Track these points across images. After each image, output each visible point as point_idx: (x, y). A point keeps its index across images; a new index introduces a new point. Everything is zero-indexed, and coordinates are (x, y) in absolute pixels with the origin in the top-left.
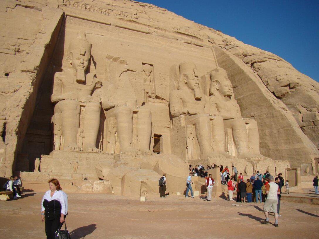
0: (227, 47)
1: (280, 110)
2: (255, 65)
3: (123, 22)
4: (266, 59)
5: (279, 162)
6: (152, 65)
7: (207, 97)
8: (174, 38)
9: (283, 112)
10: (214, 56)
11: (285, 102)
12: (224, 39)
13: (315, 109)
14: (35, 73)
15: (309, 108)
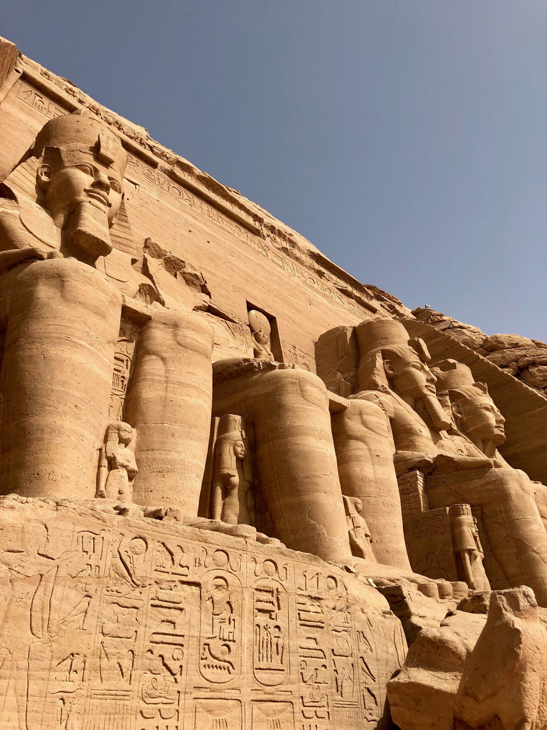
2: (534, 370)
6: (272, 319)
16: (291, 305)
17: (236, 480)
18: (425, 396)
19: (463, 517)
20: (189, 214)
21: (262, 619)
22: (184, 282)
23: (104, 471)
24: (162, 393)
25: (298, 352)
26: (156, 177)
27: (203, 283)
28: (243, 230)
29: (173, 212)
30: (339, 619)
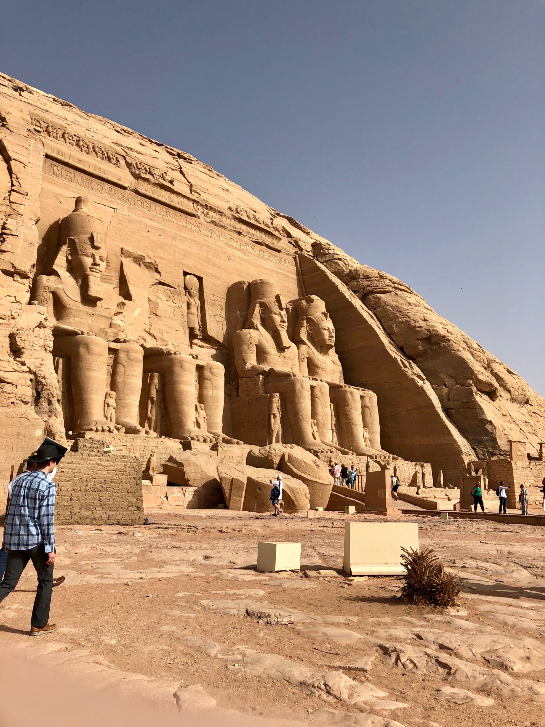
0: (320, 259)
1: (415, 378)
2: (371, 296)
3: (149, 186)
4: (391, 289)
5: (416, 465)
6: (200, 279)
7: (293, 346)
8: (234, 231)
9: (420, 383)
10: (297, 271)
11: (420, 364)
12: (316, 242)
13: (471, 382)
14: (29, 278)
15: (459, 379)
16: (215, 265)
17: (155, 399)
18: (278, 330)
19: (274, 399)
20: (148, 218)
21: (141, 452)
22: (145, 268)
23: (106, 408)
24: (123, 379)
25: (216, 298)
26: (126, 197)
27: (156, 266)
28: (184, 216)
29: (137, 220)
30: (163, 451)
